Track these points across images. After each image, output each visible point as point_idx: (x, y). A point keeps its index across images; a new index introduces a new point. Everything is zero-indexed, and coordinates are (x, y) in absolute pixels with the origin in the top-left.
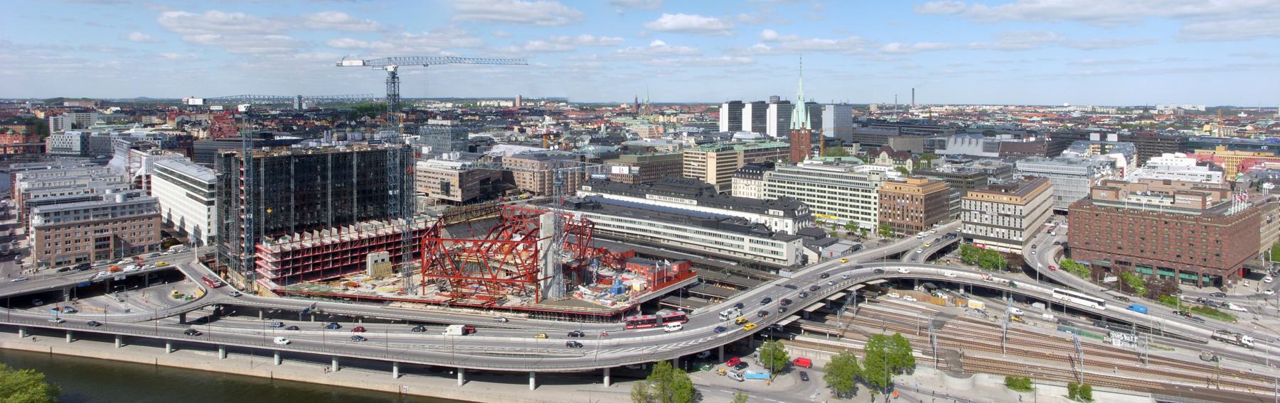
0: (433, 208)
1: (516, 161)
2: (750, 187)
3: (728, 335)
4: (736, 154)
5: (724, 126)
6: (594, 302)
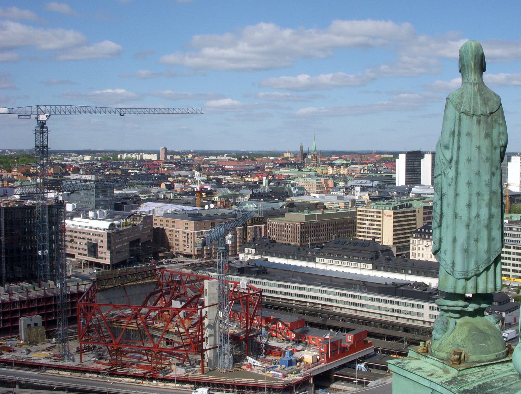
0: (80, 271)
1: (168, 221)
4: (415, 211)
5: (401, 179)
6: (264, 374)
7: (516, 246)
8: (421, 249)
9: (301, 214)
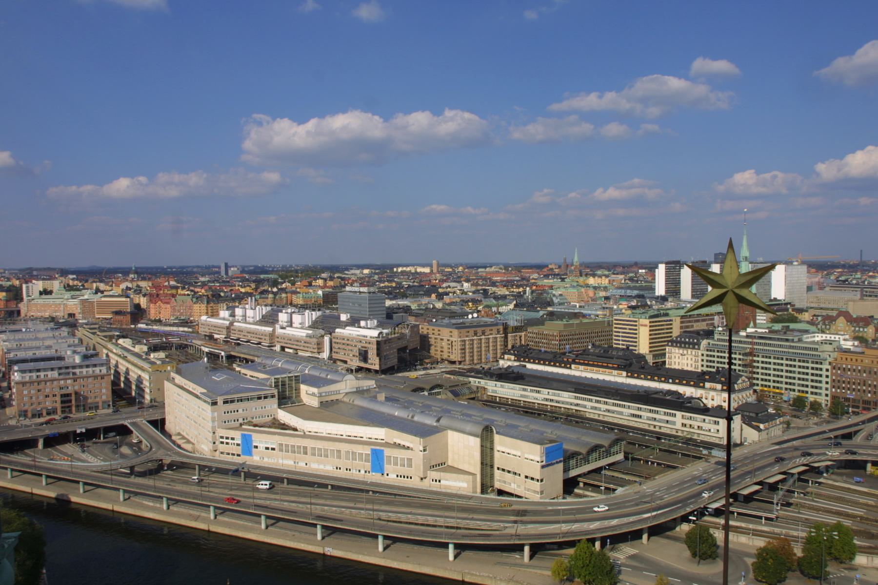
1: (433, 330)
2: (686, 357)
3: (652, 516)
4: (671, 320)
5: (660, 289)
7: (776, 356)
8: (677, 357)
9: (560, 322)
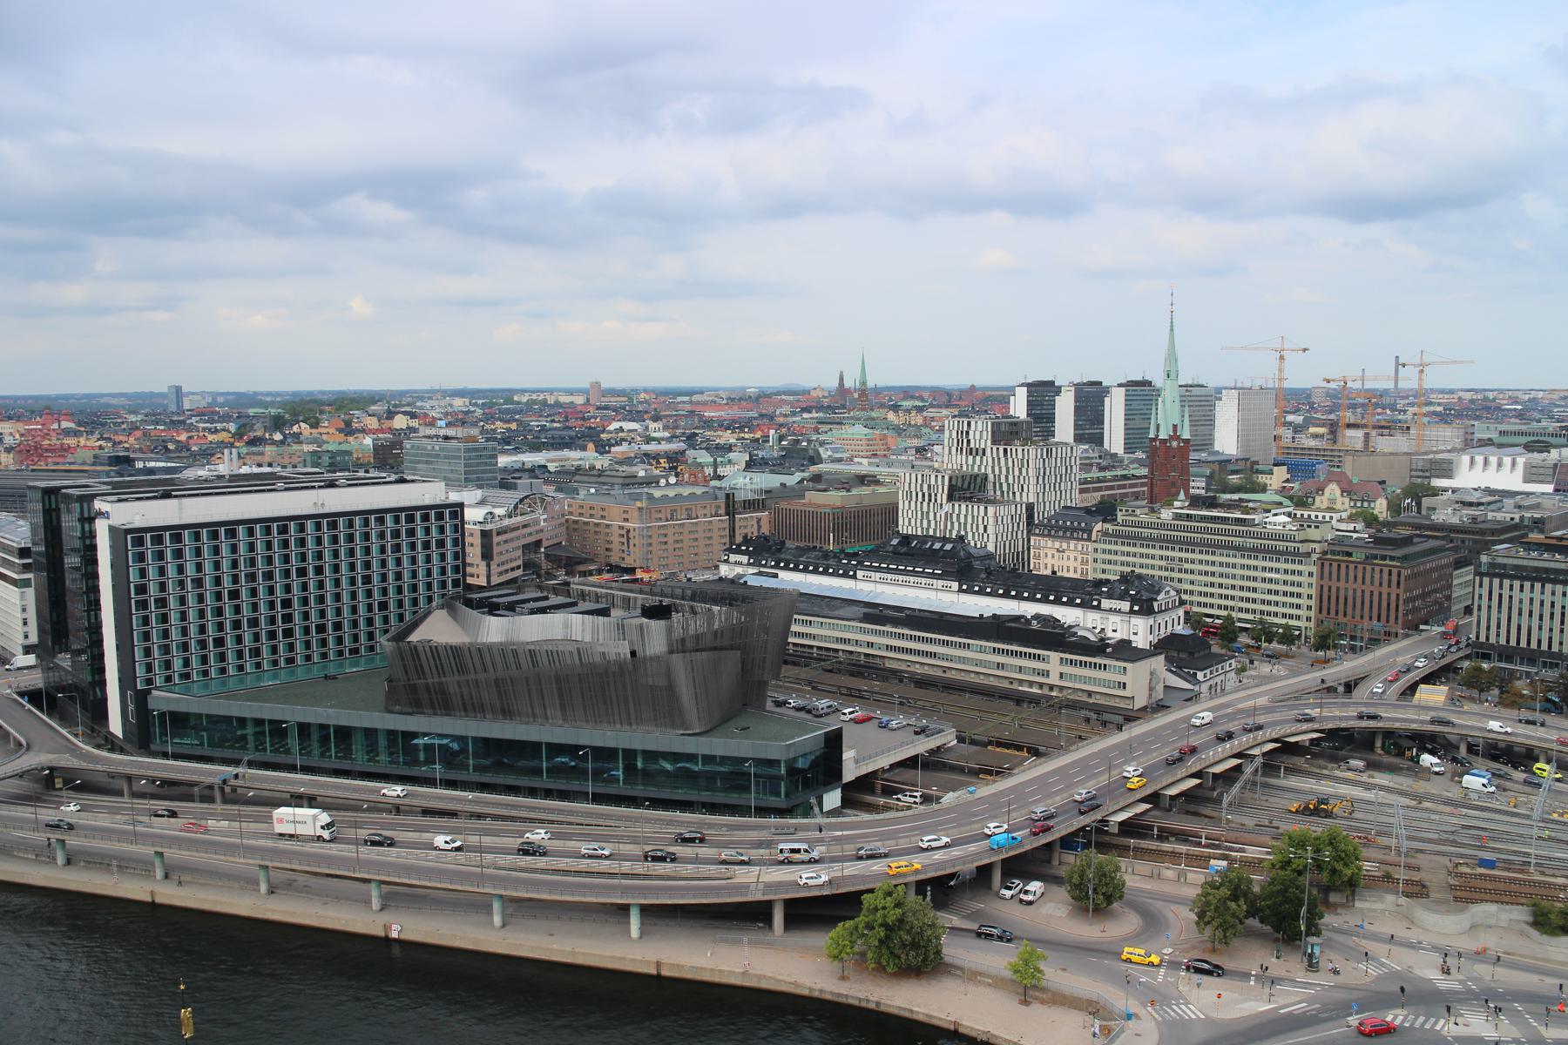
2: (1065, 555)
8: (1050, 556)
